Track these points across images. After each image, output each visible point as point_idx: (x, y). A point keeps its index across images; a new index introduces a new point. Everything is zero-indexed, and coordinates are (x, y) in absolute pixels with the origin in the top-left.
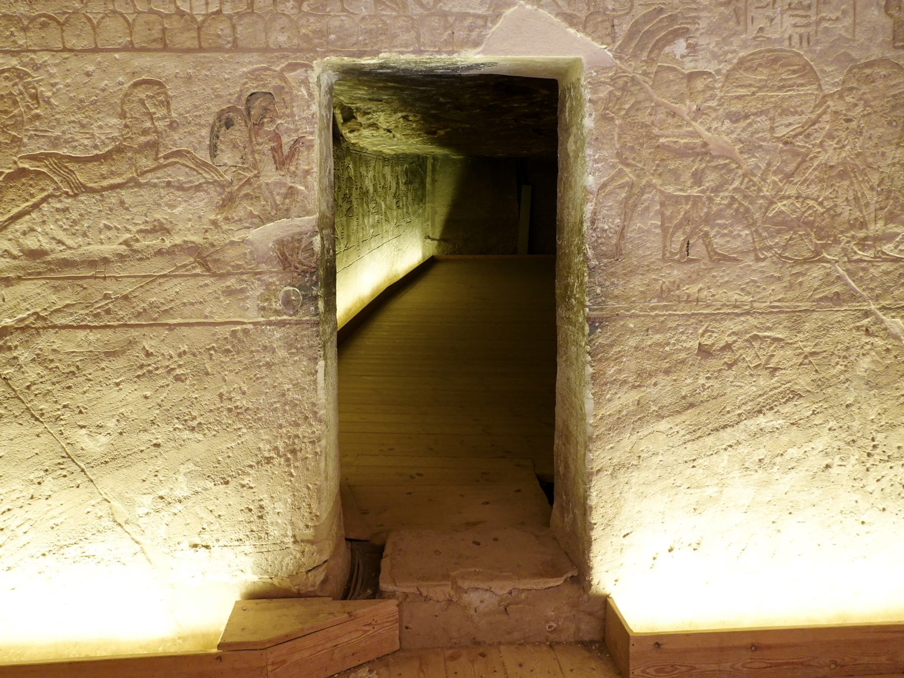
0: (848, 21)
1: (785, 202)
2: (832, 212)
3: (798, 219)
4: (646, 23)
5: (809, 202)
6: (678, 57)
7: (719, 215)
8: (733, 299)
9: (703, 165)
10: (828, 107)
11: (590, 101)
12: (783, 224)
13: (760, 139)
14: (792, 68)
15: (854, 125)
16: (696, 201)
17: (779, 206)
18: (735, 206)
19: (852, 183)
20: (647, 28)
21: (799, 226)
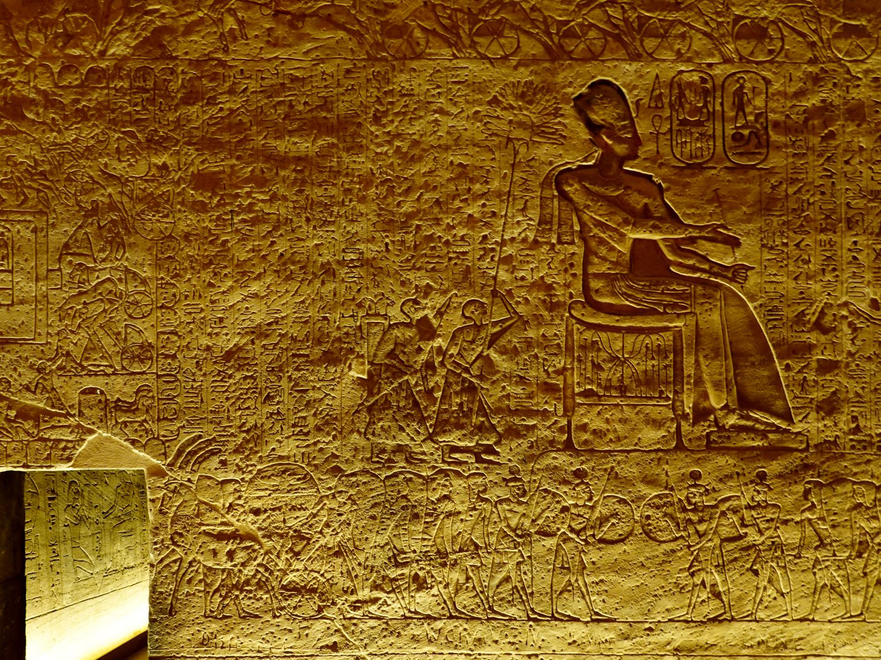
0: (337, 443)
1: (295, 574)
2: (331, 582)
3: (306, 586)
4: (189, 445)
5: (312, 573)
6: (212, 469)
7: (247, 582)
8: (256, 646)
9: (235, 546)
10: (325, 504)
11: (151, 500)
12: (295, 590)
13: (275, 527)
14: (297, 477)
15: (343, 518)
16: (230, 572)
17: (291, 577)
18: (259, 576)
19: (345, 560)
20: (190, 449)
21: (306, 592)
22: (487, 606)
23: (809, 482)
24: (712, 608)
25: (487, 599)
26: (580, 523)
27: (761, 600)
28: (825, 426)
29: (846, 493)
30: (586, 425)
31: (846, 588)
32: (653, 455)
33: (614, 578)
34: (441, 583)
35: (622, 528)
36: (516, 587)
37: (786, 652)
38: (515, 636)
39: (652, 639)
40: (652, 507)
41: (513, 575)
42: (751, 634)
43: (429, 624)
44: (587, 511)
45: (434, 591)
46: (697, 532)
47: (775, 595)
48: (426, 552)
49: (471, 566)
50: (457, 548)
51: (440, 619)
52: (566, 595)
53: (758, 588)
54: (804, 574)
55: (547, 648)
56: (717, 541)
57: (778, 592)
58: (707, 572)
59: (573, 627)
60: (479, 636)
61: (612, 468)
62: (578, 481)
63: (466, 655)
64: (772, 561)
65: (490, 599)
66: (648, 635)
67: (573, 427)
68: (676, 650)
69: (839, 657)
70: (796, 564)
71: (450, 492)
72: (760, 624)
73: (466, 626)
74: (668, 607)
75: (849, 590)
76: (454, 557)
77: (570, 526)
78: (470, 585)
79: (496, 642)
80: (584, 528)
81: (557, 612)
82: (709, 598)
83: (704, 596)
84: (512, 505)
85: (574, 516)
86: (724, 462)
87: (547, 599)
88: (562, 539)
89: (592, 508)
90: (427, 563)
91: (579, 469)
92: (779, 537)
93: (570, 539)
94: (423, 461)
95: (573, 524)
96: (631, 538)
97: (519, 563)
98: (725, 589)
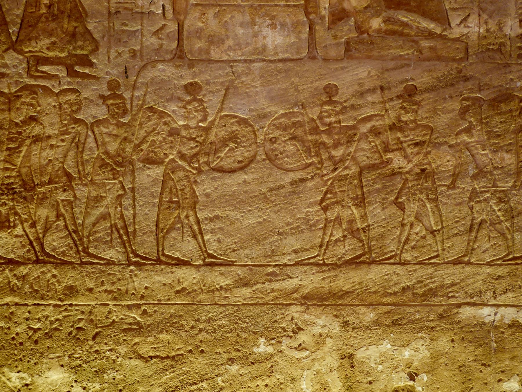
22: (80, 248)
23: (467, 99)
24: (348, 249)
25: (81, 239)
26: (192, 148)
27: (407, 239)
28: (488, 31)
29: (510, 111)
30: (202, 29)
31: (508, 225)
32: (280, 65)
33: (232, 214)
34: (26, 221)
35: (241, 153)
36: (115, 224)
37: (438, 299)
38: (113, 283)
39: (276, 285)
40: (278, 128)
41: (112, 210)
42: (395, 279)
43: (11, 270)
44: (200, 133)
45: (19, 231)
46: (331, 158)
47: (424, 233)
48: (8, 184)
49: (63, 201)
50: (46, 178)
51: (23, 264)
52: (173, 234)
53: (403, 225)
54: (458, 207)
55: (151, 297)
56: (354, 169)
57: (426, 230)
58: (343, 206)
59: (182, 272)
60: (71, 283)
61: (232, 81)
62: (189, 98)
63: (55, 306)
64: (422, 193)
65: (85, 240)
66: (271, 281)
67: (185, 33)
68: (305, 298)
69: (498, 306)
70: (449, 196)
71: (38, 112)
72: (406, 267)
73: (55, 272)
74: (295, 248)
75: (512, 226)
76: (42, 190)
77: (179, 152)
78: (61, 223)
79: (90, 290)
80: (196, 155)
81: (164, 255)
82: (344, 236)
83: (338, 234)
84: (111, 127)
85: (185, 140)
86: (365, 74)
87: (152, 239)
88: (170, 167)
89: (207, 130)
90: (10, 197)
91: (191, 84)
92: (429, 164)
93: (180, 167)
94: (3, 75)
95: (184, 150)
96: (253, 165)
97: (120, 196)
98: (363, 226)
